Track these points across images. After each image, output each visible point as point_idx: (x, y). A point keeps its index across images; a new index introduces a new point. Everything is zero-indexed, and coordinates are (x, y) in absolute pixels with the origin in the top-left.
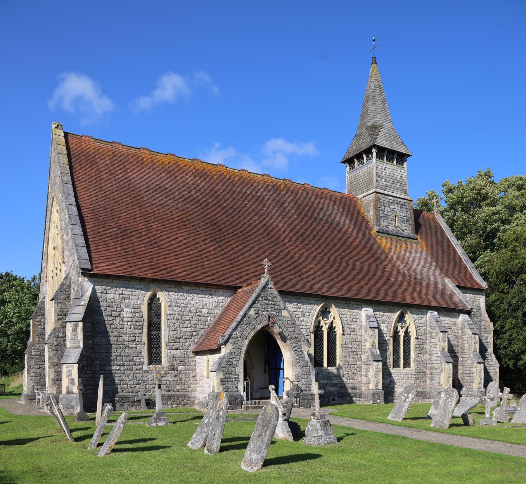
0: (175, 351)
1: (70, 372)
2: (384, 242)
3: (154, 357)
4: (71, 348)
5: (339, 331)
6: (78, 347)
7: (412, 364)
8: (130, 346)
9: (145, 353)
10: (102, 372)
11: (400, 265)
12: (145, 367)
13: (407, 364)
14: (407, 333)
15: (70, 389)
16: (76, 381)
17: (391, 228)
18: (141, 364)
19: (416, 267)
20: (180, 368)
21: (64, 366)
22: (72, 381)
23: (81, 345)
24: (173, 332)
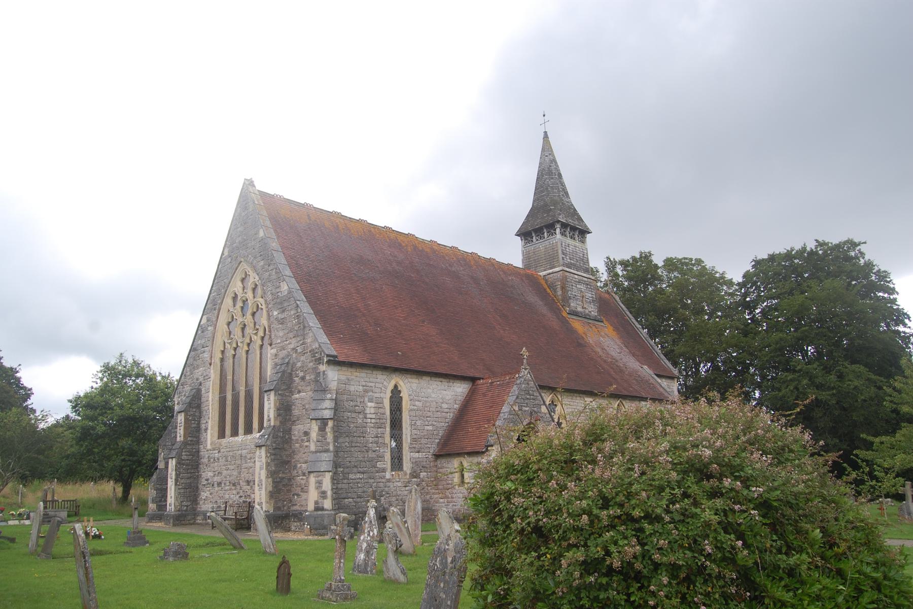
1: (319, 483)
2: (577, 324)
4: (316, 452)
6: (327, 451)
8: (374, 449)
9: (388, 457)
10: (345, 481)
11: (599, 350)
12: (388, 475)
15: (320, 505)
16: (329, 493)
17: (579, 309)
18: (384, 470)
19: (613, 354)
20: (423, 474)
21: (312, 475)
22: (323, 494)
23: (331, 448)
24: (415, 432)
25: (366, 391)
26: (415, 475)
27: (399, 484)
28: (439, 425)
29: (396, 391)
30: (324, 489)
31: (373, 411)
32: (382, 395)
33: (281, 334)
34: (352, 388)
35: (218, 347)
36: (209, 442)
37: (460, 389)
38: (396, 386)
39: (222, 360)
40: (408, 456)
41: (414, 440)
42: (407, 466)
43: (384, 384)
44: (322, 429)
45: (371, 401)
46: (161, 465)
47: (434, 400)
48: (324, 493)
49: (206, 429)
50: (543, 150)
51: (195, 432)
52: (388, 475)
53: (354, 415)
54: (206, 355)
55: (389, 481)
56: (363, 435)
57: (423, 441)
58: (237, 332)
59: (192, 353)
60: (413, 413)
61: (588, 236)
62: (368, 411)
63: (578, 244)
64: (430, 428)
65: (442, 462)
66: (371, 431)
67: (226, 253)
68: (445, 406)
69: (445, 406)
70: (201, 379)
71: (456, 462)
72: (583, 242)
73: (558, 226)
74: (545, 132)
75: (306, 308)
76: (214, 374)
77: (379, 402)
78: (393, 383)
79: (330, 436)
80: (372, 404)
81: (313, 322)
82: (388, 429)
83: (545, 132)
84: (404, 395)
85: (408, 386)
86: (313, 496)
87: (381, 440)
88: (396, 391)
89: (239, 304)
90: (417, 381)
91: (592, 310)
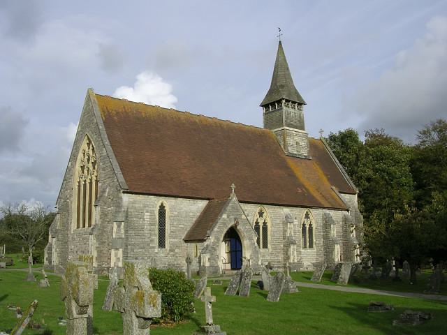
0: (173, 240)
2: (291, 162)
3: (162, 244)
5: (269, 225)
7: (314, 246)
9: (156, 239)
13: (311, 246)
14: (310, 225)
16: (121, 259)
24: (172, 228)
25: (145, 207)
26: (171, 251)
27: (163, 255)
28: (187, 225)
29: (162, 207)
30: (119, 256)
31: (148, 217)
32: (154, 209)
33: (103, 176)
37: (202, 204)
38: (162, 204)
39: (79, 186)
40: (168, 241)
43: (156, 202)
44: (119, 226)
45: (147, 212)
46: (50, 241)
47: (188, 210)
48: (119, 259)
49: (71, 223)
51: (66, 225)
52: (156, 251)
53: (137, 219)
55: (157, 253)
56: (142, 229)
58: (86, 171)
59: (65, 182)
60: (172, 218)
62: (145, 217)
63: (297, 111)
64: (182, 226)
67: (80, 129)
69: (191, 214)
73: (284, 101)
74: (280, 42)
75: (115, 163)
77: (152, 213)
79: (123, 231)
80: (148, 214)
81: (118, 170)
82: (157, 227)
83: (280, 42)
84: (167, 208)
85: (169, 203)
86: (113, 259)
87: (153, 233)
88: (162, 207)
89: (87, 157)
90: (174, 201)
91: (305, 152)
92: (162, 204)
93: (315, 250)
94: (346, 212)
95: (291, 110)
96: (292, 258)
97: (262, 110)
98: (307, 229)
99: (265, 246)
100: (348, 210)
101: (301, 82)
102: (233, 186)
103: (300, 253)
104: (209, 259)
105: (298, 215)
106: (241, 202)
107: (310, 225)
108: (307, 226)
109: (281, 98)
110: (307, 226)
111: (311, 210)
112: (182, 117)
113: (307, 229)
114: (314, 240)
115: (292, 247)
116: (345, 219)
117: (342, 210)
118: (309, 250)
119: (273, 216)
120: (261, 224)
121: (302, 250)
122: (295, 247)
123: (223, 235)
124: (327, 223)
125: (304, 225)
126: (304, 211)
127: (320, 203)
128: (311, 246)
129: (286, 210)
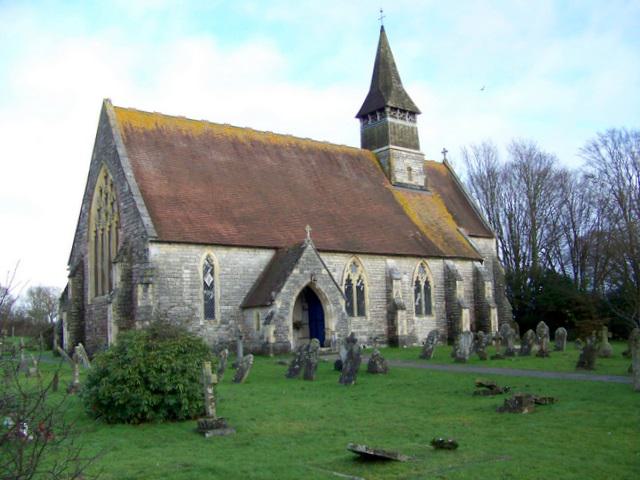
0: (226, 307)
2: (399, 194)
3: (210, 313)
7: (433, 312)
14: (427, 283)
20: (231, 322)
26: (223, 322)
34: (171, 260)
35: (93, 229)
36: (89, 300)
37: (265, 256)
38: (208, 256)
39: (96, 237)
40: (219, 309)
41: (224, 296)
42: (218, 316)
45: (187, 268)
50: (380, 43)
52: (201, 323)
54: (85, 234)
56: (181, 293)
57: (232, 297)
58: (103, 216)
61: (418, 117)
62: (184, 276)
64: (238, 287)
65: (246, 312)
66: (187, 291)
68: (251, 270)
69: (251, 270)
70: (83, 252)
71: (255, 312)
72: (415, 122)
74: (382, 27)
76: (91, 247)
77: (194, 270)
78: (205, 254)
83: (382, 27)
85: (218, 255)
87: (196, 297)
88: (208, 259)
91: (420, 181)
92: (208, 259)
93: (434, 318)
94: (478, 264)
95: (399, 122)
96: (400, 328)
97: (358, 123)
98: (423, 288)
99: (361, 312)
100: (481, 261)
101: (413, 84)
102: (308, 229)
103: (413, 322)
104: (275, 333)
105: (407, 270)
106: (319, 250)
107: (427, 283)
108: (423, 284)
109: (384, 103)
110: (423, 284)
111: (427, 261)
112: (240, 135)
113: (423, 288)
114: (433, 304)
115: (400, 313)
116: (477, 274)
117: (472, 260)
118: (426, 319)
119: (371, 270)
120: (355, 283)
121: (416, 318)
122: (404, 312)
123: (294, 298)
124: (450, 279)
125: (418, 282)
126: (418, 263)
127: (441, 252)
128: (429, 312)
129: (391, 262)
